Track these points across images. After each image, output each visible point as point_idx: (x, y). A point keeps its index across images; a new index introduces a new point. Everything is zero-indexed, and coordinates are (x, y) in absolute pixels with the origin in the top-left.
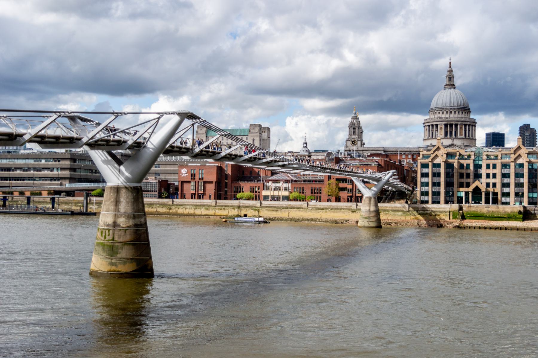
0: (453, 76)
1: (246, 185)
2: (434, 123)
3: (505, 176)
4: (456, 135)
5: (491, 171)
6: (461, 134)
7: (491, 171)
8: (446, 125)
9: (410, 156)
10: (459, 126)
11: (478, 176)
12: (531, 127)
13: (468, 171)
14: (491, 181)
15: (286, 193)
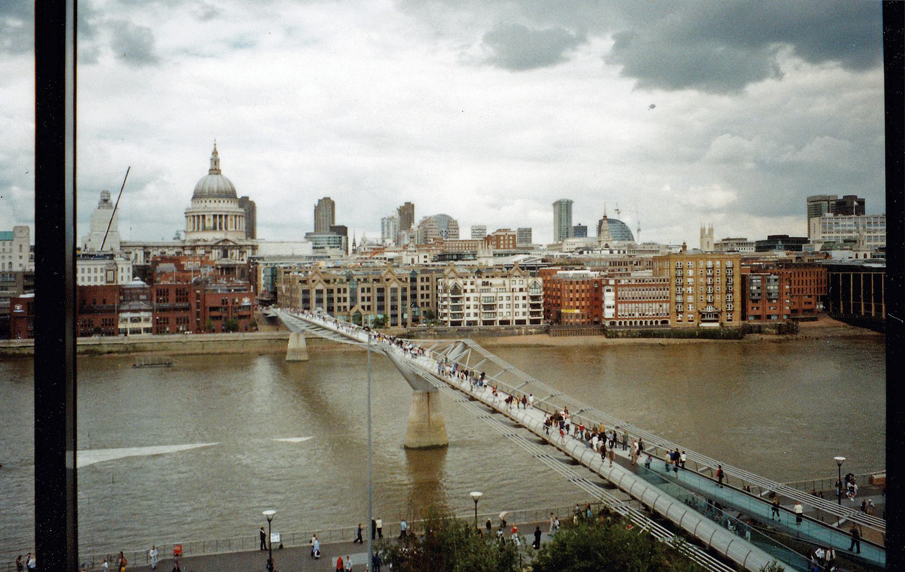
0: (219, 160)
1: (98, 320)
2: (200, 214)
3: (381, 299)
4: (226, 228)
5: (366, 295)
6: (231, 227)
7: (366, 295)
8: (215, 216)
9: (198, 259)
10: (229, 218)
11: (354, 299)
12: (250, 199)
13: (345, 295)
14: (366, 303)
15: (149, 325)
